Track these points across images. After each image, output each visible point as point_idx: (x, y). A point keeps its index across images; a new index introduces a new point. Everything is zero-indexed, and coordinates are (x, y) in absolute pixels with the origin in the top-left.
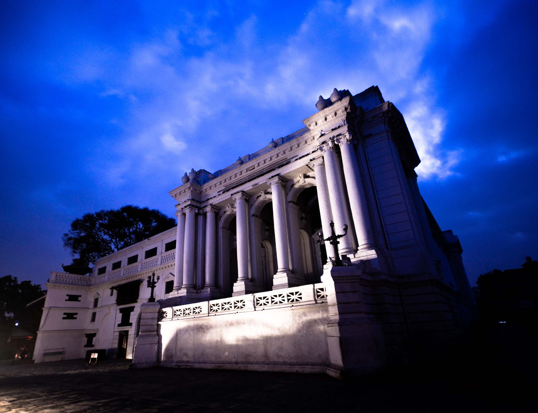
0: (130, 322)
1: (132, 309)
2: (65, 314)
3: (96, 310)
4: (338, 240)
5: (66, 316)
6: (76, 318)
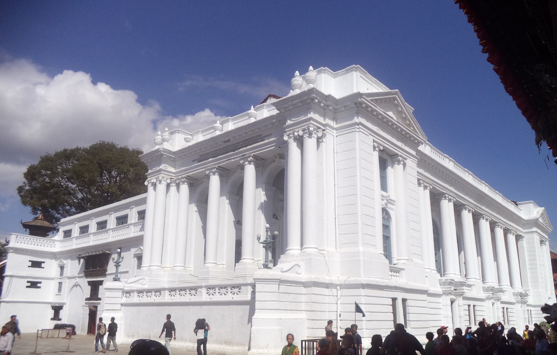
0: (99, 296)
1: (101, 283)
2: (28, 282)
5: (29, 284)
6: (40, 287)
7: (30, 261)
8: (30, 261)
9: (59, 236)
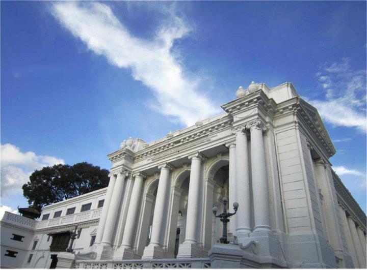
2: (7, 251)
3: (34, 253)
4: (228, 218)
5: (8, 253)
6: (15, 257)
7: (13, 234)
8: (13, 234)
9: (40, 219)
